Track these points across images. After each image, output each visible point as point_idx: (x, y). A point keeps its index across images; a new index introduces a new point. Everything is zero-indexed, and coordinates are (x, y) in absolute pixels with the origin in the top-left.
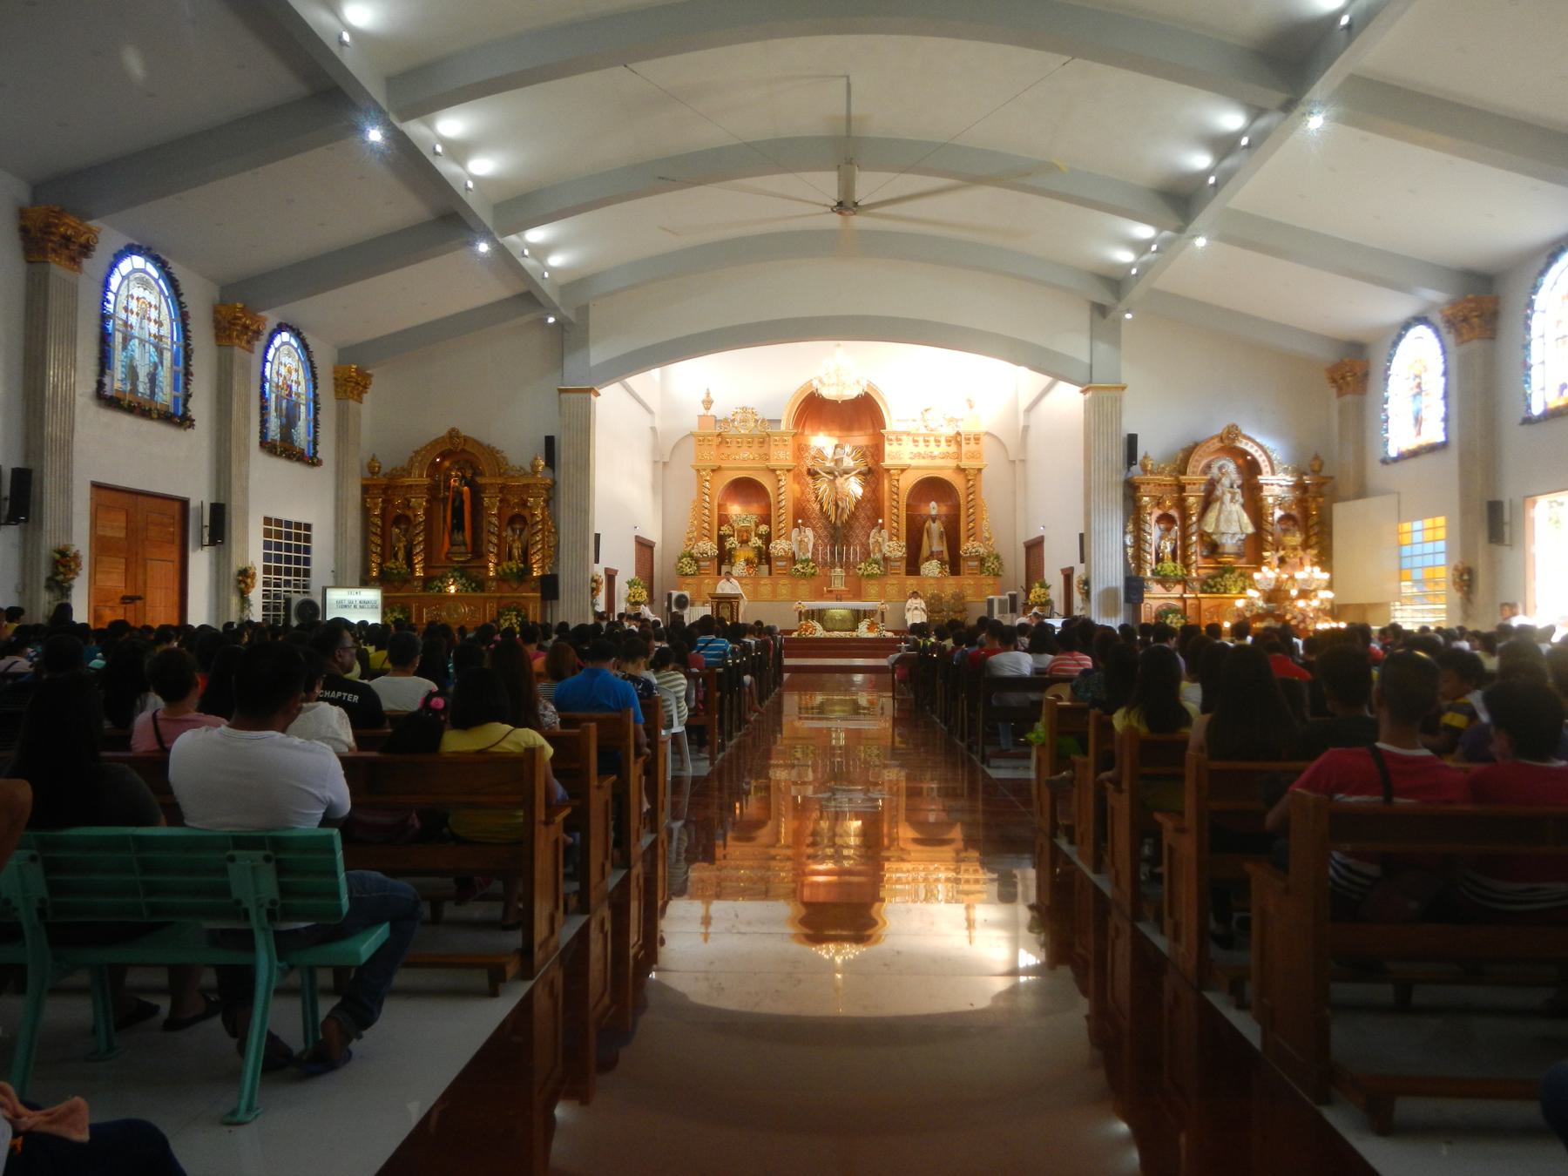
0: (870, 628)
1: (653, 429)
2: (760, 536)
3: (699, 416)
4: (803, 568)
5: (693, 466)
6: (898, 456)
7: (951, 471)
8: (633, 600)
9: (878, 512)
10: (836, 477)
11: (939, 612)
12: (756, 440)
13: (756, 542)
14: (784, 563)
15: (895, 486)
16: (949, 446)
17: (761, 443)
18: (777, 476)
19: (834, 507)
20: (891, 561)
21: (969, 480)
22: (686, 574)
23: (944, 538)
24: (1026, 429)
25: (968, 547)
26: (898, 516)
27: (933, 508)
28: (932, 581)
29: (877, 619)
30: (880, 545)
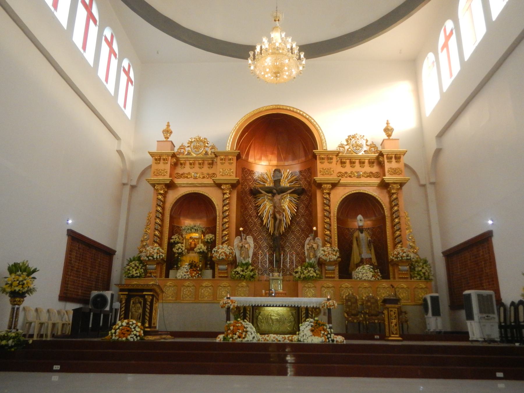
0: (314, 331)
1: (120, 152)
2: (206, 243)
3: (158, 141)
4: (243, 271)
5: (148, 181)
6: (328, 172)
7: (375, 188)
8: (9, 290)
9: (311, 220)
10: (274, 195)
11: (376, 315)
12: (206, 162)
13: (201, 247)
14: (225, 267)
15: (326, 199)
16: (373, 166)
17: (209, 164)
18: (223, 190)
19: (273, 221)
20: (325, 264)
21: (393, 194)
22: (133, 276)
23: (372, 246)
24: (438, 152)
25: (393, 253)
26: (330, 225)
27: (360, 221)
28: (366, 284)
29: (322, 318)
30: (315, 251)
